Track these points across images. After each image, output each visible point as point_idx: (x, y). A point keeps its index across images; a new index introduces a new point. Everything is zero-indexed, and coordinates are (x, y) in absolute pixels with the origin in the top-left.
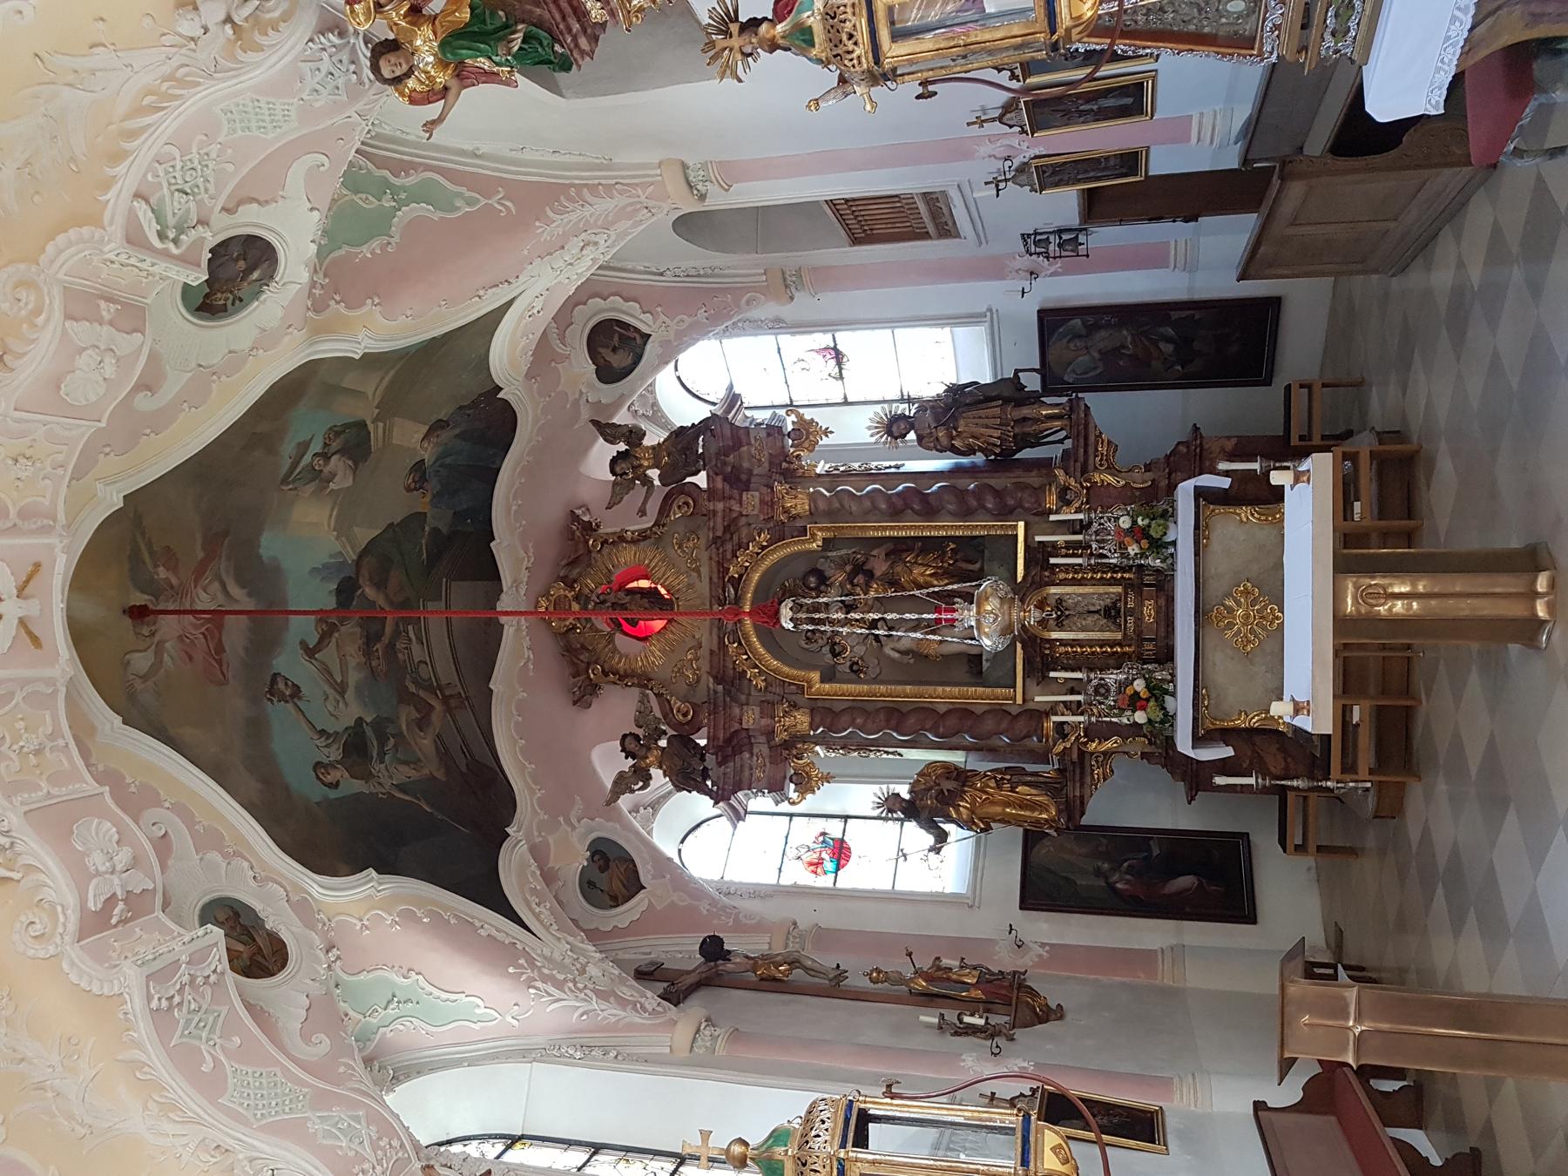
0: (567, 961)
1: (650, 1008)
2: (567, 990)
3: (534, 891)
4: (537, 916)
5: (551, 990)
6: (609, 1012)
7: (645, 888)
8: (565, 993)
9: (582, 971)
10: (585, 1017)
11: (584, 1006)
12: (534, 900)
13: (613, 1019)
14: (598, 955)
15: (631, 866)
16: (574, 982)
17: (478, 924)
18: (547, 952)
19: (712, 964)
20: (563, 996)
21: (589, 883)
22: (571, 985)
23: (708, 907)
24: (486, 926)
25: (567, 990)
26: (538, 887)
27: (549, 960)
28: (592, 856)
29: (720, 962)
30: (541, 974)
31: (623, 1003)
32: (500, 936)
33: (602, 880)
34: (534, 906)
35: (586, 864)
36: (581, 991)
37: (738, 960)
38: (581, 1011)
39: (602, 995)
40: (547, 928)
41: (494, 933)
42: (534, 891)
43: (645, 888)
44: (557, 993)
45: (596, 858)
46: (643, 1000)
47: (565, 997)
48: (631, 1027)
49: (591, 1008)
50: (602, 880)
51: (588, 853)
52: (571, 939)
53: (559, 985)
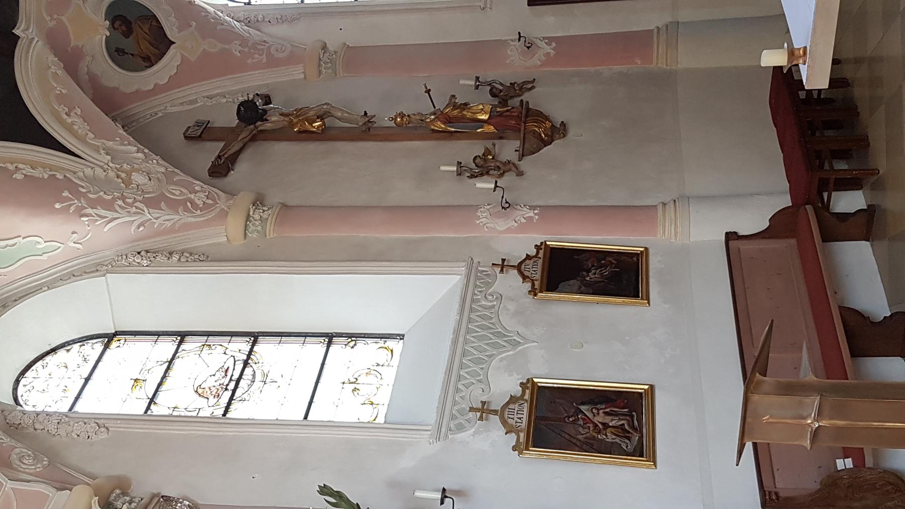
0: (112, 174)
1: (200, 203)
2: (118, 208)
3: (61, 98)
4: (69, 128)
5: (103, 212)
6: (163, 218)
7: (174, 43)
8: (117, 212)
9: (128, 182)
10: (141, 229)
11: (138, 219)
12: (62, 110)
13: (169, 224)
14: (140, 155)
15: (154, 23)
16: (123, 198)
17: (11, 167)
18: (88, 171)
19: (252, 126)
20: (116, 215)
21: (118, 50)
22: (120, 202)
23: (240, 48)
24: (20, 166)
25: (118, 208)
26: (63, 91)
27: (92, 180)
28: (112, 24)
29: (259, 123)
30: (88, 199)
31: (174, 205)
32: (37, 173)
33: (128, 44)
34: (65, 117)
35: (108, 34)
36: (131, 205)
37: (274, 119)
38: (136, 224)
39: (152, 203)
40: (82, 140)
41: (29, 171)
42: (61, 98)
43: (174, 43)
44: (110, 214)
45: (117, 24)
46: (192, 196)
47: (118, 215)
48: (187, 227)
49: (145, 219)
50: (128, 44)
51: (107, 22)
52: (110, 144)
53: (109, 206)
